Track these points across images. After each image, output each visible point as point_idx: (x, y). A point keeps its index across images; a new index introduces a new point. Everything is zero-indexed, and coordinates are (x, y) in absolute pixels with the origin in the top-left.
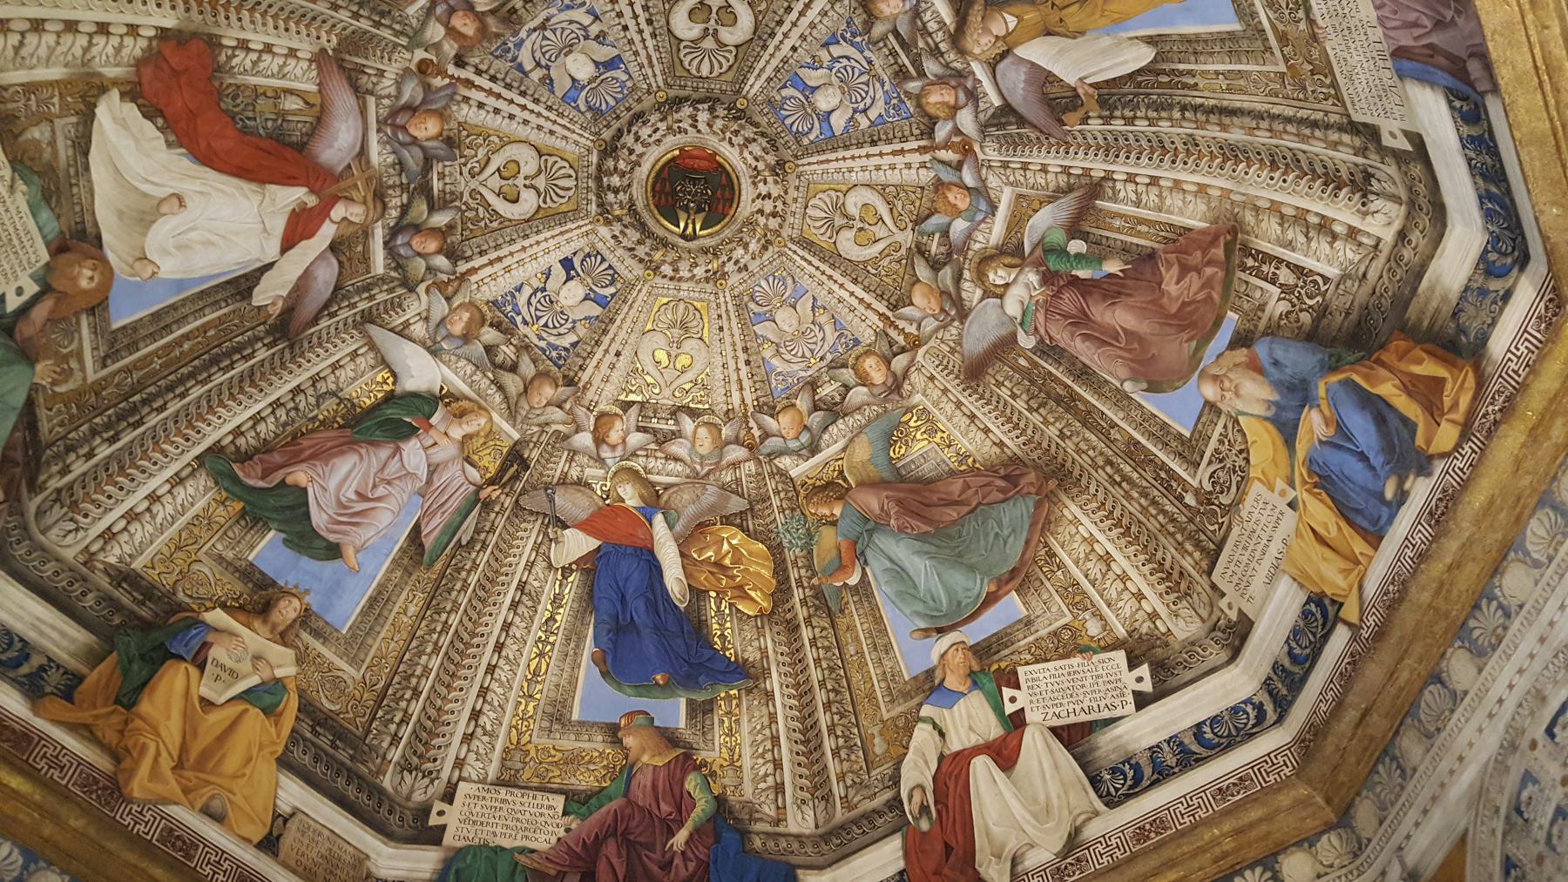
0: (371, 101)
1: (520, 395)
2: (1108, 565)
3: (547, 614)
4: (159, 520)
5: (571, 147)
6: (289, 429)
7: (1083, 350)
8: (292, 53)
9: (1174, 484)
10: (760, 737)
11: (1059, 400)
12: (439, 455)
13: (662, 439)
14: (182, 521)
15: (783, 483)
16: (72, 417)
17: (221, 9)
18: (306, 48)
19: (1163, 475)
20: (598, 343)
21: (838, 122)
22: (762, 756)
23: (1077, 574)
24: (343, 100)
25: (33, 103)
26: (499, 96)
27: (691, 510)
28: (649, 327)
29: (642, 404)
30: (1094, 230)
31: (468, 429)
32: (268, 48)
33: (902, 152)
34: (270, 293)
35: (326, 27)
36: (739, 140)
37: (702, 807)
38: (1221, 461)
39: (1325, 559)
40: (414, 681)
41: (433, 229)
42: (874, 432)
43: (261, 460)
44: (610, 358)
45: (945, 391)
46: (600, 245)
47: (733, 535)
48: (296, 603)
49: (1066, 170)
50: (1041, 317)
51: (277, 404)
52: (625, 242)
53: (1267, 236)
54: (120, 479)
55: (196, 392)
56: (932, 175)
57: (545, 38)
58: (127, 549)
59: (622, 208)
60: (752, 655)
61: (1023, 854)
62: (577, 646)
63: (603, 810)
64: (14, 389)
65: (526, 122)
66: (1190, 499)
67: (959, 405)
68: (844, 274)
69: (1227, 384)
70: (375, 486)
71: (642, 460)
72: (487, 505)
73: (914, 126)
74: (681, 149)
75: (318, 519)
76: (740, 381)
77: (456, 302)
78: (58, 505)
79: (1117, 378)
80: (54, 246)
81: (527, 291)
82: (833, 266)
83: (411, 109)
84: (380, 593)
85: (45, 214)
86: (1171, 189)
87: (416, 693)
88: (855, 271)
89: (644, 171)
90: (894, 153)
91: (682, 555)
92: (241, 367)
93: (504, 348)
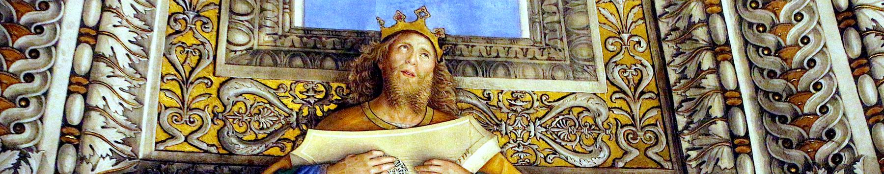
4: (123, 60)
14: (156, 41)
40: (701, 33)
48: (418, 43)
54: (21, 41)
58: (113, 135)
87: (720, 51)
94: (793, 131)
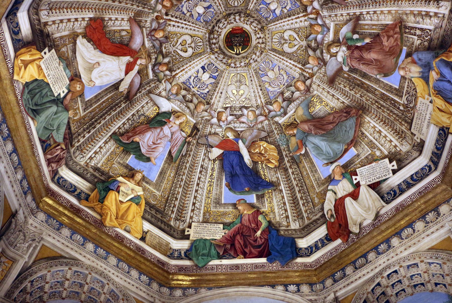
0: (144, 29)
1: (194, 109)
2: (380, 134)
3: (211, 174)
4: (103, 153)
5: (200, 33)
6: (133, 126)
7: (363, 68)
8: (123, 19)
9: (396, 104)
10: (279, 203)
11: (358, 85)
12: (174, 129)
13: (238, 117)
14: (108, 154)
15: (277, 125)
16: (79, 126)
17: (104, 10)
18: (126, 17)
19: (393, 102)
20: (215, 90)
21: (278, 12)
22: (281, 208)
23: (371, 138)
24: (137, 30)
25: (62, 41)
26: (178, 22)
27: (250, 138)
28: (230, 83)
29: (231, 107)
30: (360, 31)
31: (181, 121)
32: (116, 19)
33: (298, 17)
34: (123, 87)
35: (131, 11)
36: (249, 23)
37: (264, 224)
38: (409, 94)
39: (442, 116)
40: (175, 195)
41: (164, 63)
42: (303, 105)
43: (127, 135)
44: (219, 94)
45: (323, 89)
46: (212, 61)
47: (264, 144)
48: (140, 174)
49: (348, 14)
50: (349, 60)
51: (128, 119)
52: (219, 59)
53: (411, 22)
55: (108, 118)
56: (308, 23)
57: (189, 3)
58: (96, 161)
59: (217, 48)
60: (274, 179)
61: (363, 222)
62: (221, 182)
63: (235, 227)
64: (64, 119)
65: (187, 28)
66: (401, 108)
67: (328, 92)
68: (287, 57)
69: (407, 69)
70: (157, 140)
71: (233, 124)
72: (189, 143)
73: (301, 9)
74: (232, 28)
75: (143, 151)
76: (260, 96)
77: (173, 84)
78: (78, 151)
79: (375, 75)
80: (70, 79)
81: (193, 78)
82: (283, 56)
83: (155, 30)
84: (162, 171)
85: (67, 71)
86: (380, 14)
87: (176, 199)
88: (290, 56)
89: (222, 37)
90: (296, 18)
91: (249, 152)
92: (118, 110)
93: (188, 95)
94: (180, 214)
